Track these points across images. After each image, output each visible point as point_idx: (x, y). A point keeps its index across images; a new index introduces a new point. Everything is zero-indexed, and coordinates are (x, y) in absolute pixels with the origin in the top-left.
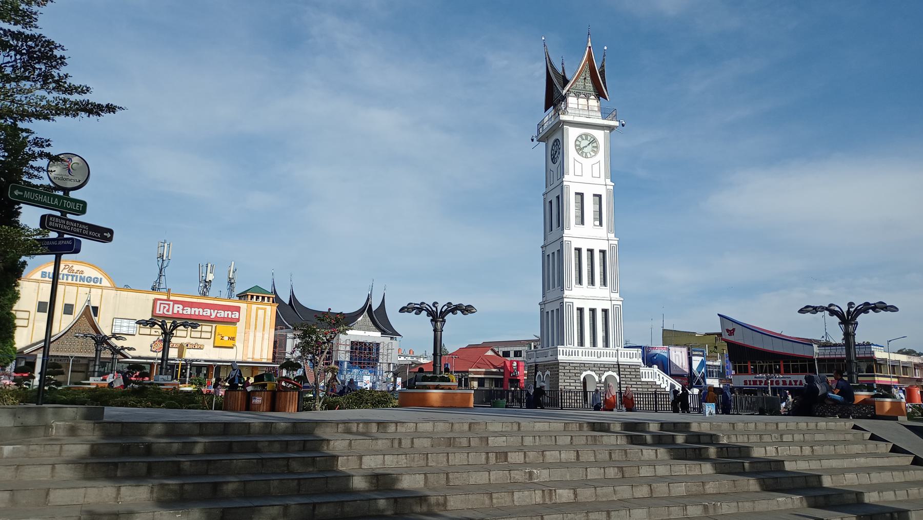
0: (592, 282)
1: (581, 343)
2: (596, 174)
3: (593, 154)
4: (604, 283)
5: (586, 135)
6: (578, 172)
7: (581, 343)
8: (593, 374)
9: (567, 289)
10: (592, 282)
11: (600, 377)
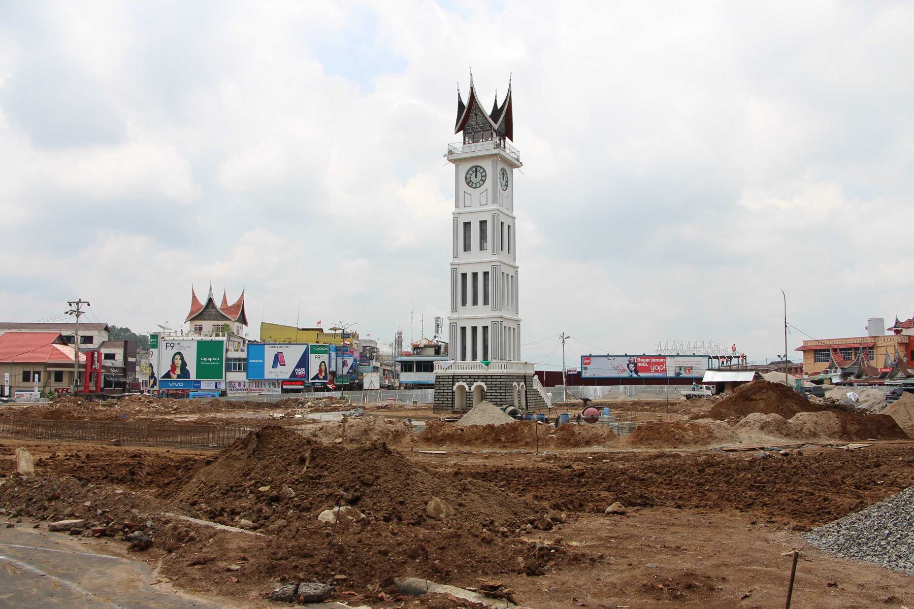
0: (475, 302)
1: (464, 357)
2: (484, 202)
3: (481, 183)
4: (486, 302)
5: (476, 167)
6: (468, 203)
7: (464, 357)
8: (464, 384)
9: (493, 309)
10: (475, 302)
11: (470, 387)
